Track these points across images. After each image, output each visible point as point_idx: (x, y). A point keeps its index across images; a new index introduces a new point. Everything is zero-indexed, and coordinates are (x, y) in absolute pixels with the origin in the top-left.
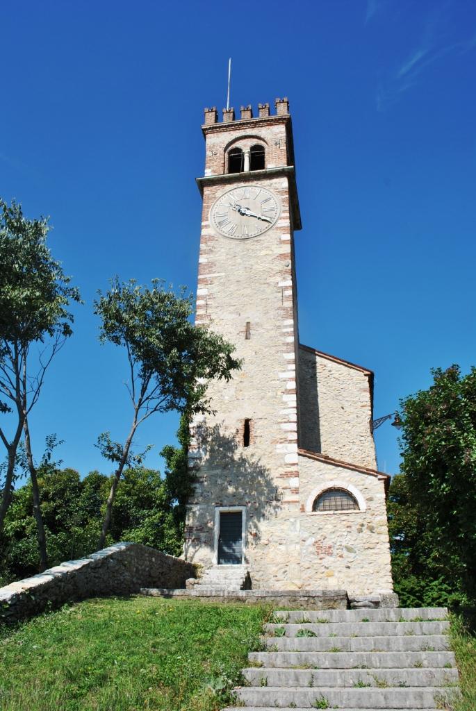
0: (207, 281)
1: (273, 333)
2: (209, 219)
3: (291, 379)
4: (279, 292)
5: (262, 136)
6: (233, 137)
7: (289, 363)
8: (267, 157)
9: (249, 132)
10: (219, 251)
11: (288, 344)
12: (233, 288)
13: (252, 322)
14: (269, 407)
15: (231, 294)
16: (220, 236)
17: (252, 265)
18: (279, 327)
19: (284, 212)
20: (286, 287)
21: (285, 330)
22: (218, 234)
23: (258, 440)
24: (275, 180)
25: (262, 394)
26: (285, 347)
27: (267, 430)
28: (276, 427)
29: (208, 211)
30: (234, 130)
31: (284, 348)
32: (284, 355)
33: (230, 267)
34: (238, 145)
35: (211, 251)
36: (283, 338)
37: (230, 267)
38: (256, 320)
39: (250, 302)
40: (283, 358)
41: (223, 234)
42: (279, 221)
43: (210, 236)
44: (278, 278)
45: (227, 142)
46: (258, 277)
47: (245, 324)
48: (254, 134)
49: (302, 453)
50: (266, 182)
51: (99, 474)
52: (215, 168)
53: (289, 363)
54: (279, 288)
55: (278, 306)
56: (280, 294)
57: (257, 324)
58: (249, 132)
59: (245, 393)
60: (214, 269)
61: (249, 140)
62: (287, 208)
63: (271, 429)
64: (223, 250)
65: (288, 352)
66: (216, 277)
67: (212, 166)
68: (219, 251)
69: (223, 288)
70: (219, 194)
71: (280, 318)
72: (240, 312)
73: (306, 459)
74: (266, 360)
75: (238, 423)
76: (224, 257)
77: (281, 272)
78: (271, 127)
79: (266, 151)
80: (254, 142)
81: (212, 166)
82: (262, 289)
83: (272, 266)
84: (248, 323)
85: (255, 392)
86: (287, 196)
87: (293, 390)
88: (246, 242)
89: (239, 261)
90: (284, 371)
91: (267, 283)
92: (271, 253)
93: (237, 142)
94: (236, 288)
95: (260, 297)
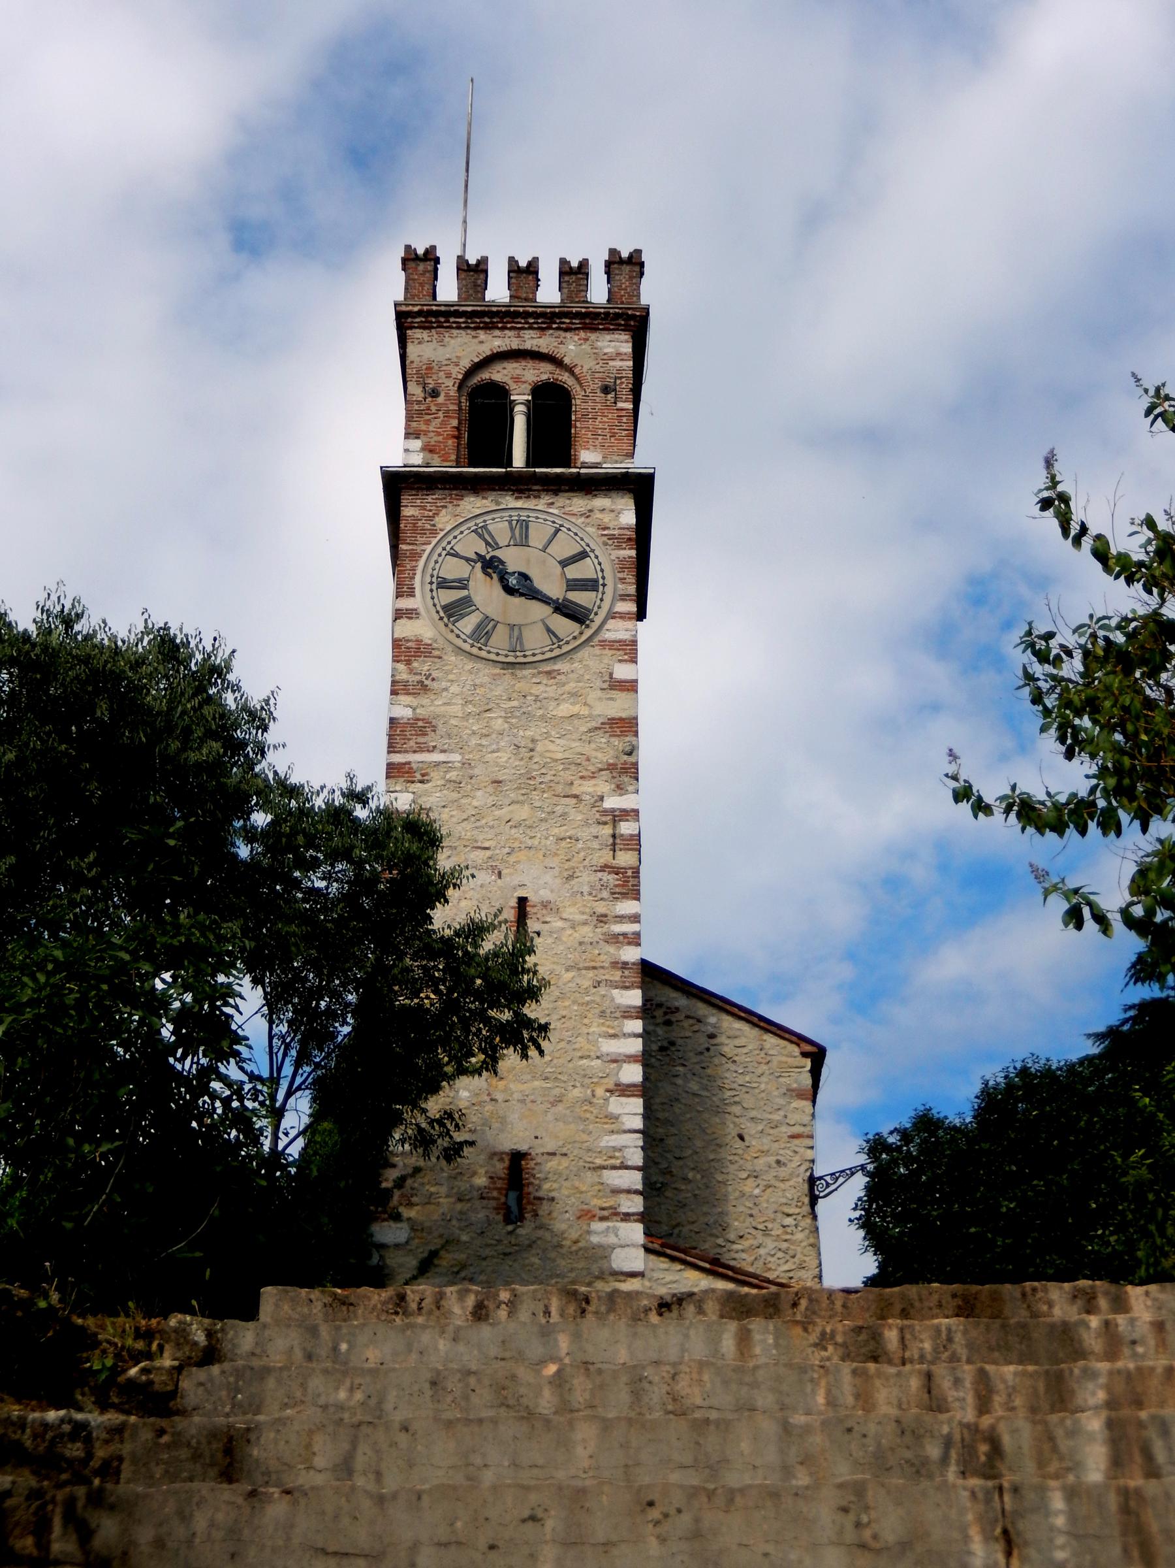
0: (411, 772)
1: (587, 932)
2: (418, 592)
3: (630, 1059)
4: (605, 823)
5: (567, 360)
6: (486, 350)
7: (627, 1014)
8: (580, 429)
9: (531, 340)
10: (446, 689)
11: (625, 965)
12: (481, 798)
13: (533, 898)
14: (572, 1126)
15: (478, 816)
16: (449, 649)
17: (533, 741)
18: (602, 919)
19: (624, 597)
20: (624, 811)
21: (618, 928)
22: (441, 641)
23: (545, 1208)
24: (601, 502)
25: (557, 1091)
26: (619, 973)
27: (566, 1184)
28: (590, 1177)
29: (414, 569)
30: (488, 327)
31: (617, 975)
32: (616, 992)
33: (474, 741)
34: (500, 374)
35: (425, 688)
36: (611, 949)
37: (474, 741)
38: (542, 892)
39: (529, 843)
40: (613, 1000)
41: (459, 642)
42: (611, 624)
43: (419, 641)
44: (602, 786)
45: (466, 364)
46: (548, 778)
47: (513, 903)
48: (544, 350)
49: (656, 1246)
50: (579, 503)
51: (862, 1194)
52: (434, 439)
53: (627, 1014)
54: (605, 812)
55: (602, 861)
56: (607, 831)
57: (545, 905)
58: (531, 340)
59: (512, 1086)
60: (431, 740)
61: (530, 364)
62: (632, 589)
63: (577, 1184)
64: (454, 689)
65: (627, 988)
66: (437, 764)
67: (426, 433)
68: (446, 689)
69: (455, 795)
70: (445, 521)
71: (605, 894)
72: (501, 867)
73: (662, 1263)
74: (567, 1003)
75: (495, 1161)
76: (456, 709)
77: (611, 767)
78: (593, 336)
79: (577, 403)
80: (543, 372)
81: (426, 433)
82: (559, 809)
83: (588, 749)
84: (522, 901)
85: (537, 1083)
86: (633, 553)
87: (634, 1085)
88: (519, 673)
89: (498, 724)
90: (614, 1036)
91: (576, 796)
92: (585, 711)
93: (498, 366)
94: (490, 801)
95: (556, 831)
